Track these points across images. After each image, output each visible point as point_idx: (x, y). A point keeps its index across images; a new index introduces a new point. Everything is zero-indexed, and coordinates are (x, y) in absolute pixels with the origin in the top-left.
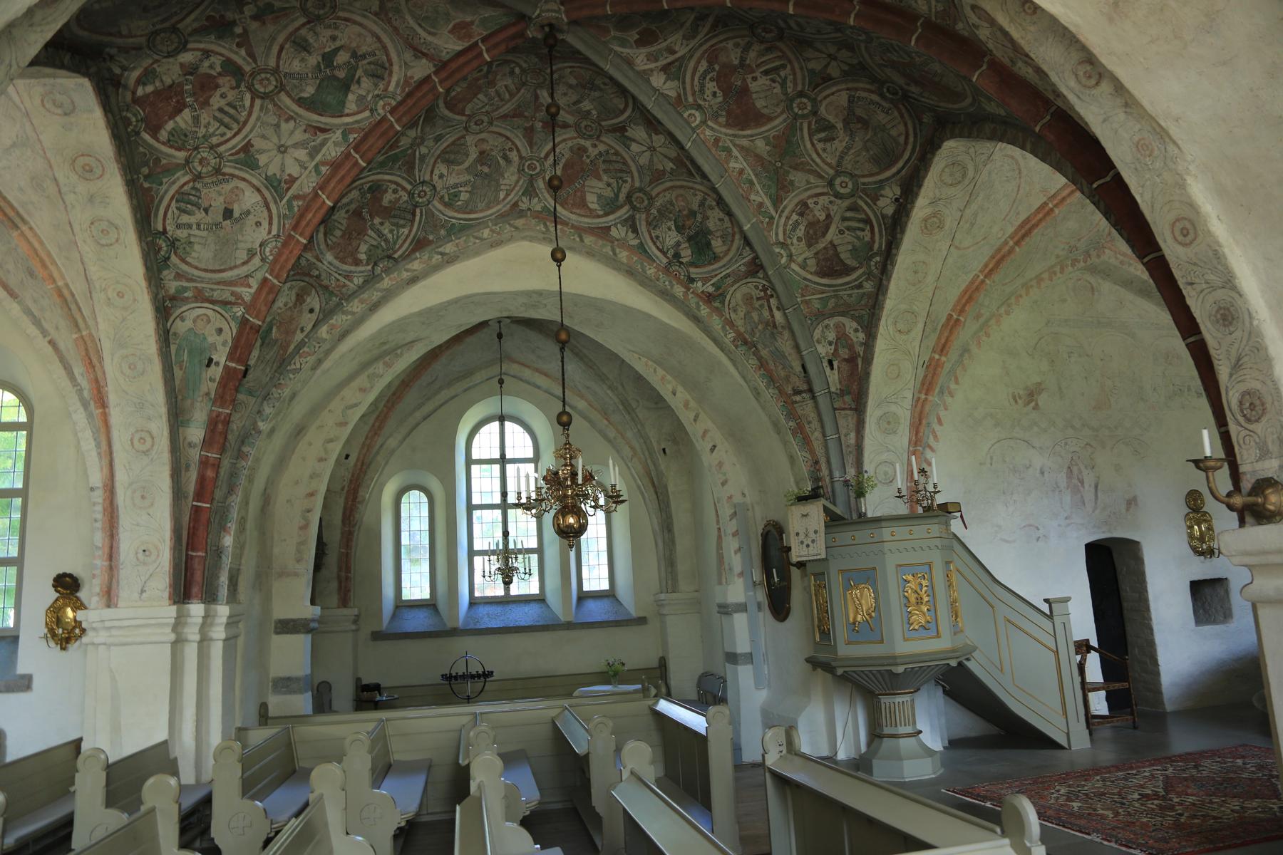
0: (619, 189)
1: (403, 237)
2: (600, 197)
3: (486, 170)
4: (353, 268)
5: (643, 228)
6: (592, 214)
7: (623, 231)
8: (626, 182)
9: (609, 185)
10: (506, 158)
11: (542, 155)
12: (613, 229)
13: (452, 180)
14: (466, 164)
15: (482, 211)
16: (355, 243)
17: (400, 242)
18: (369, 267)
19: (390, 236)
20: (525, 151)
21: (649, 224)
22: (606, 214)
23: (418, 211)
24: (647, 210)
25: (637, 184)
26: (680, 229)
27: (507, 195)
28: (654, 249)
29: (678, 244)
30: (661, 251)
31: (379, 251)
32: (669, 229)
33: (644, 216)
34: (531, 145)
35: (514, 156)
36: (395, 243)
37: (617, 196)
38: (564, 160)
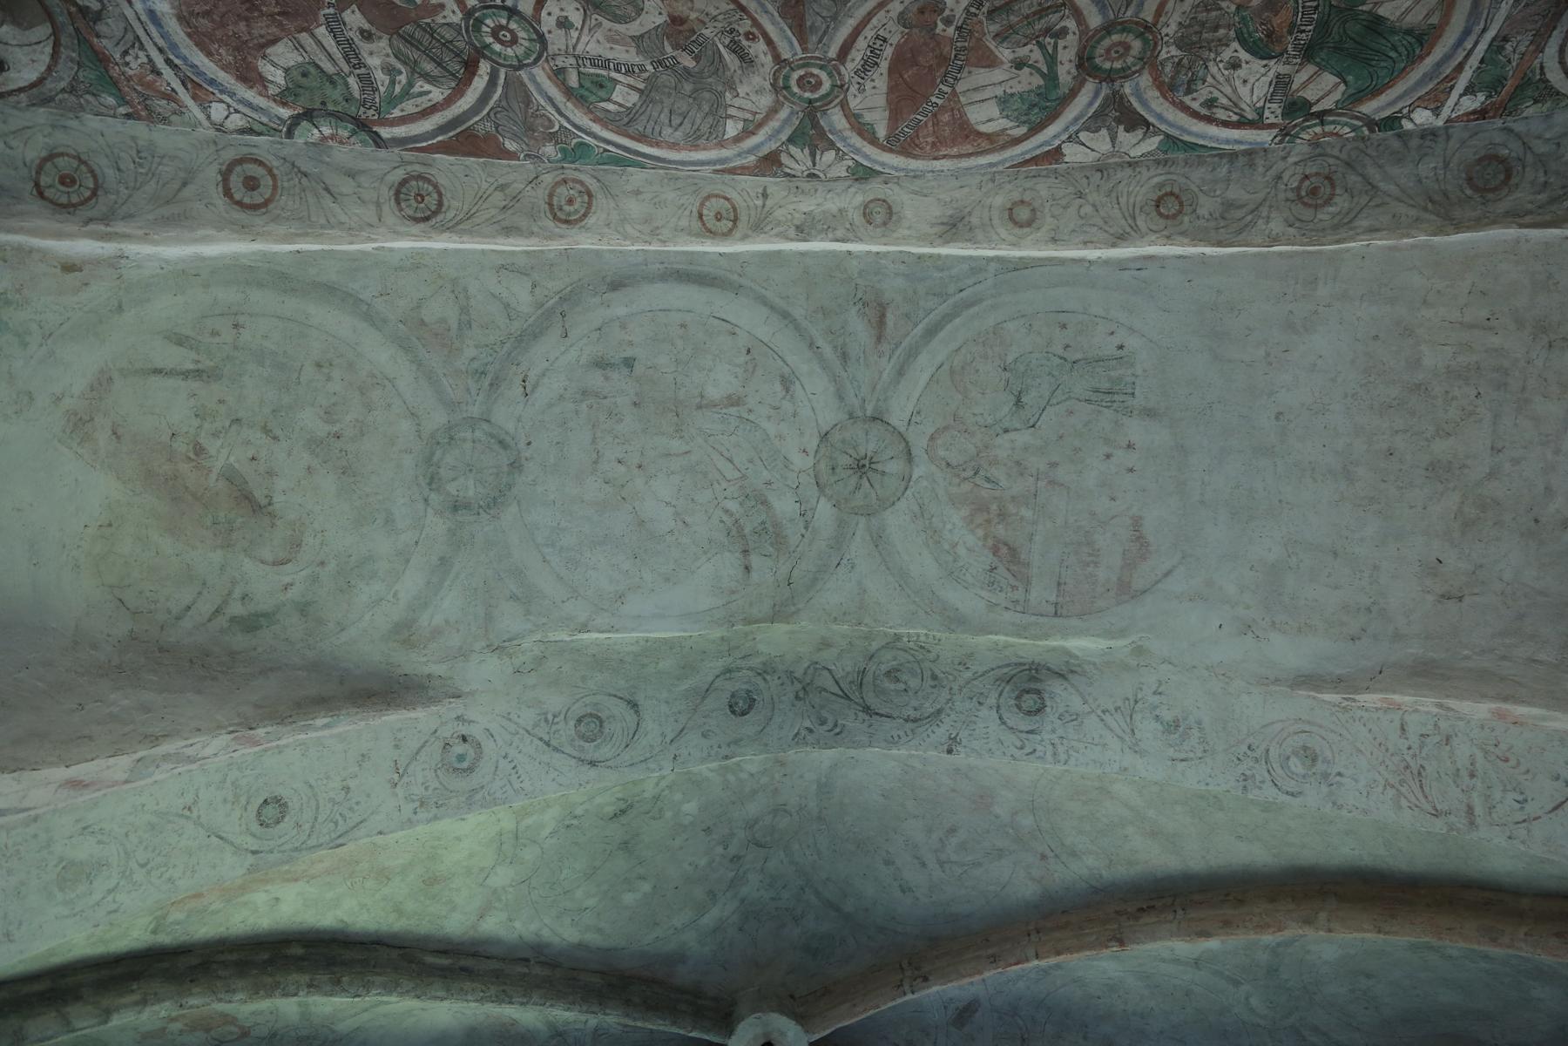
0: (1052, 60)
1: (424, 103)
2: (1004, 101)
3: (687, 61)
4: (224, 77)
5: (1156, 106)
6: (995, 142)
7: (1101, 142)
8: (1063, 32)
9: (1019, 64)
10: (736, 48)
11: (833, 52)
12: (1067, 149)
13: (593, 45)
14: (635, 28)
15: (673, 146)
16: (261, 28)
17: (409, 107)
18: (286, 113)
19: (381, 78)
20: (789, 48)
21: (1167, 89)
22: (1035, 129)
23: (484, 67)
24: (1149, 61)
25: (1095, 20)
26: (1262, 50)
27: (747, 133)
28: (1213, 130)
29: (1282, 83)
30: (1242, 124)
31: (336, 94)
32: (1235, 65)
33: (1145, 80)
34: (801, 31)
35: (758, 48)
36: (393, 101)
37: (1051, 78)
38: (889, 52)
